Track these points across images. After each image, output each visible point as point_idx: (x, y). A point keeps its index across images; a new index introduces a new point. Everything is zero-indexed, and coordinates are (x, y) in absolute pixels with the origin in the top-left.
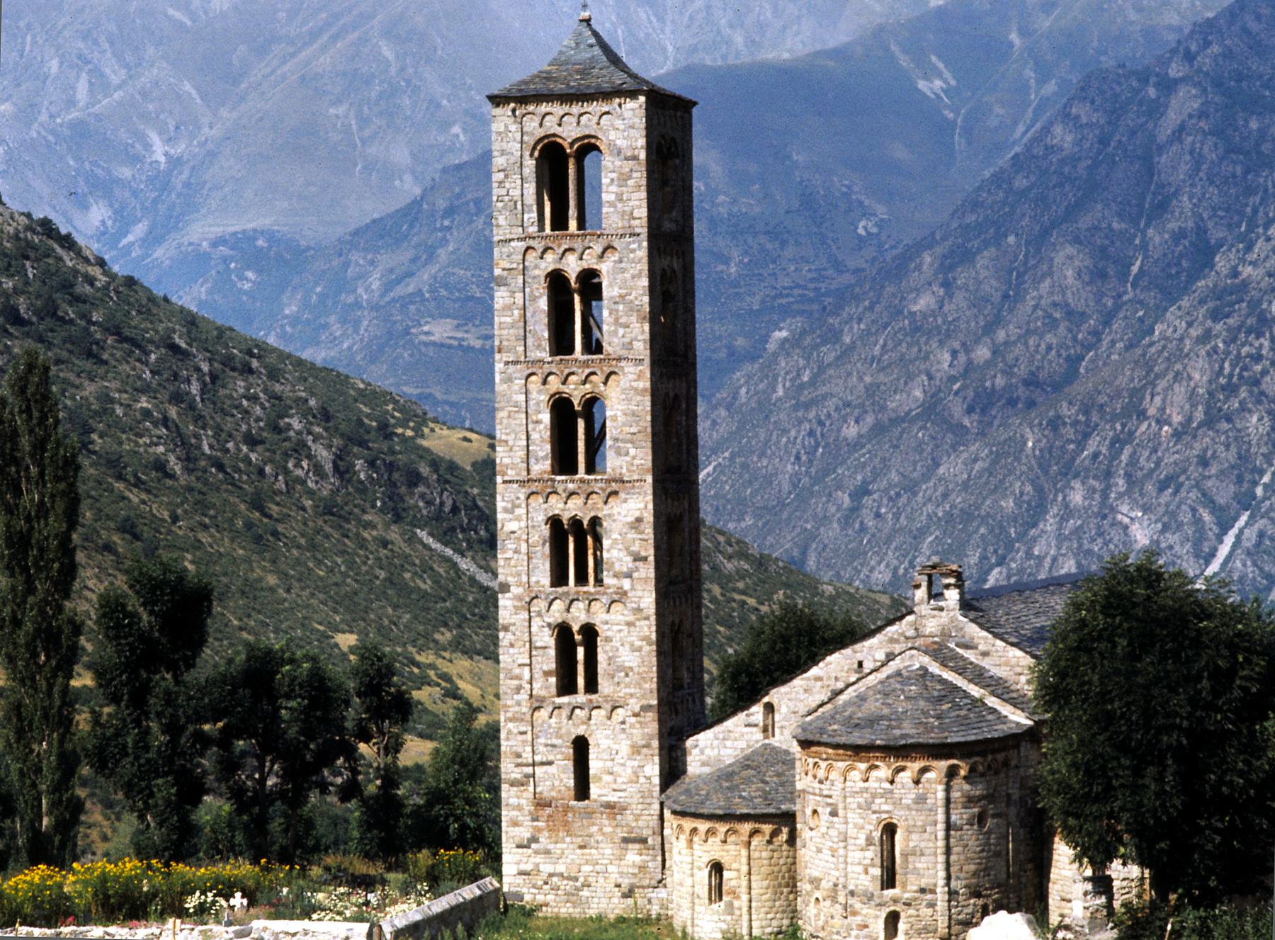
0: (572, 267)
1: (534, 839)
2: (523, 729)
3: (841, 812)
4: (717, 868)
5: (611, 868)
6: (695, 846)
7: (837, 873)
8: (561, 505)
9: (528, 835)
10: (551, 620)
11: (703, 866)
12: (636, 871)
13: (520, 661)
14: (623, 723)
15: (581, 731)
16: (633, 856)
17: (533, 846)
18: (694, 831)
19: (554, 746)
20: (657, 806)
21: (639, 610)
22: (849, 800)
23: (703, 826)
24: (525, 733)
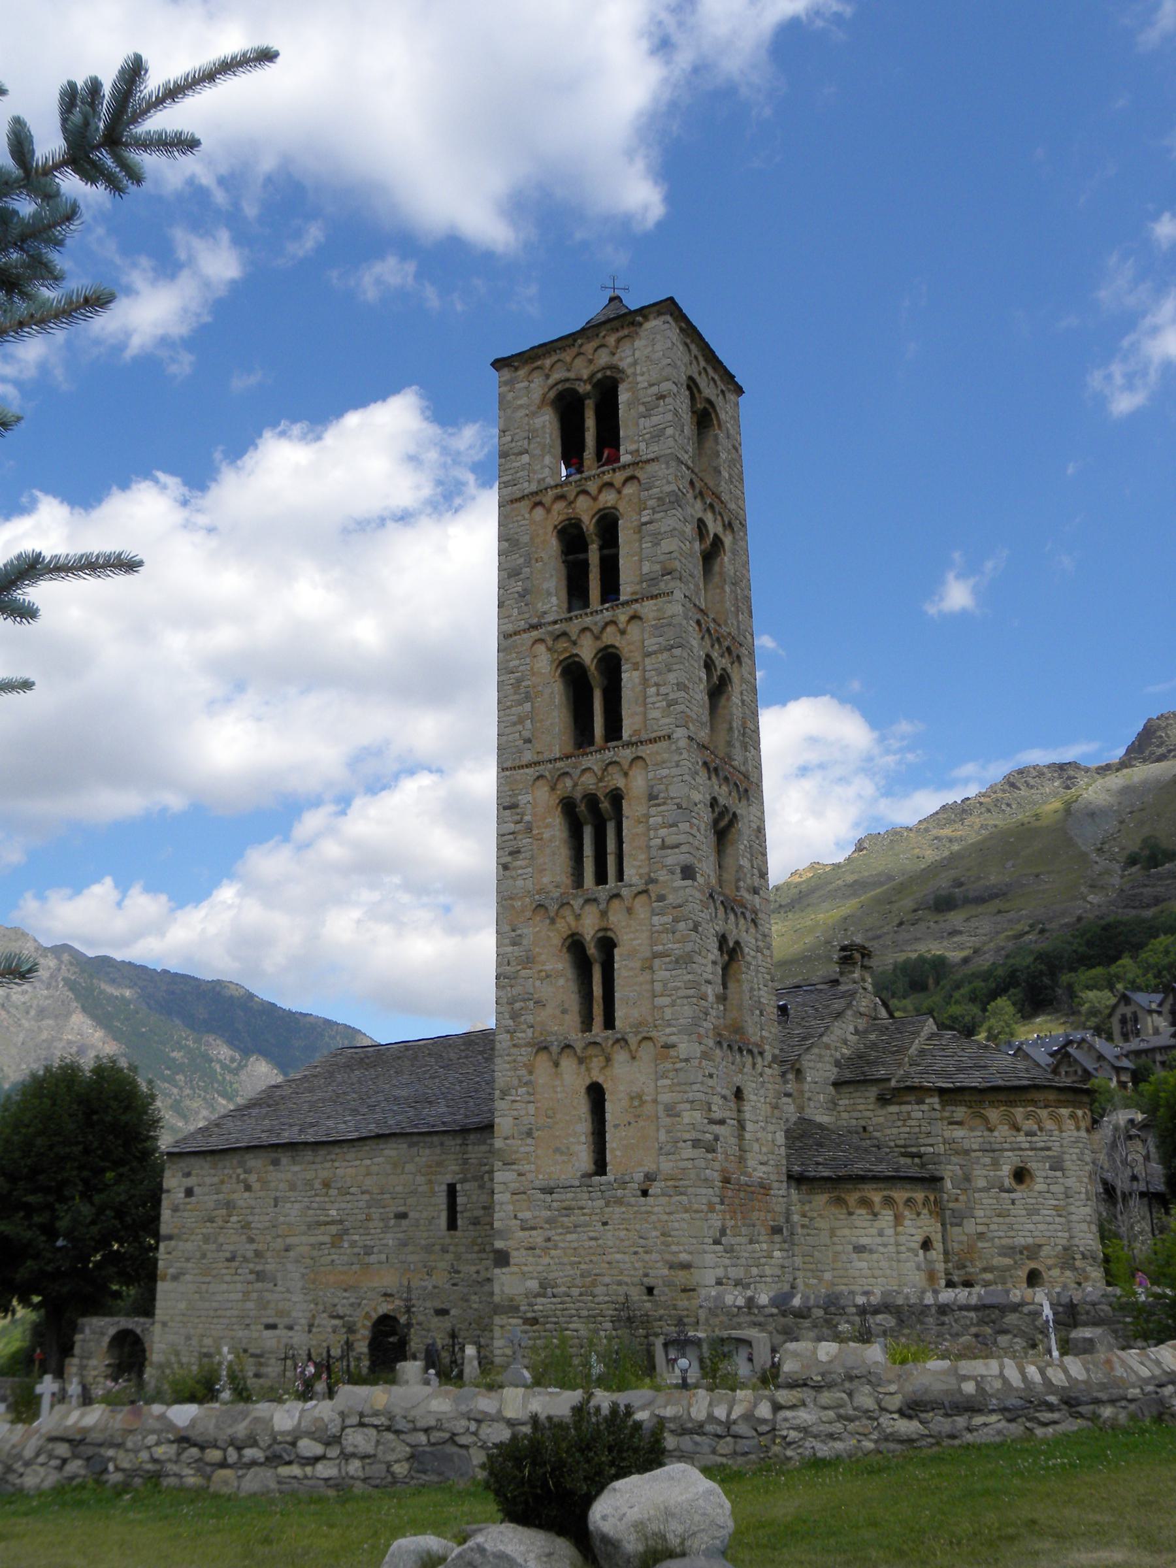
0: (714, 527)
1: (723, 1232)
2: (713, 1071)
3: (1068, 1164)
4: (926, 1245)
5: (768, 1270)
6: (907, 1222)
7: (1066, 1235)
8: (717, 787)
9: (719, 1223)
10: (717, 928)
11: (916, 1246)
12: (779, 1273)
13: (705, 976)
14: (761, 1075)
15: (738, 1080)
16: (777, 1254)
17: (724, 1240)
18: (909, 1202)
19: (724, 1097)
20: (785, 1185)
21: (765, 936)
22: (1072, 1150)
23: (919, 1196)
24: (711, 1076)
